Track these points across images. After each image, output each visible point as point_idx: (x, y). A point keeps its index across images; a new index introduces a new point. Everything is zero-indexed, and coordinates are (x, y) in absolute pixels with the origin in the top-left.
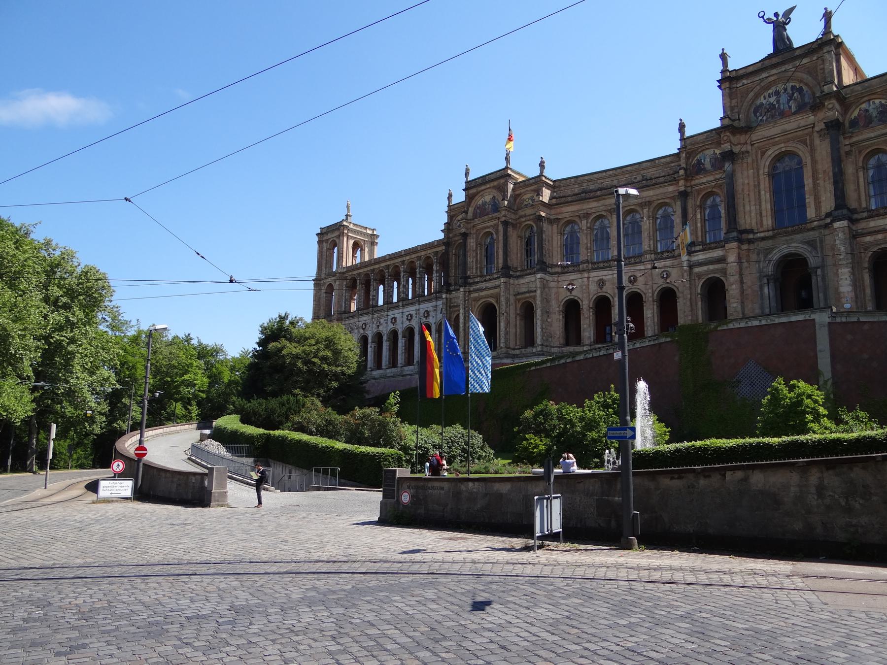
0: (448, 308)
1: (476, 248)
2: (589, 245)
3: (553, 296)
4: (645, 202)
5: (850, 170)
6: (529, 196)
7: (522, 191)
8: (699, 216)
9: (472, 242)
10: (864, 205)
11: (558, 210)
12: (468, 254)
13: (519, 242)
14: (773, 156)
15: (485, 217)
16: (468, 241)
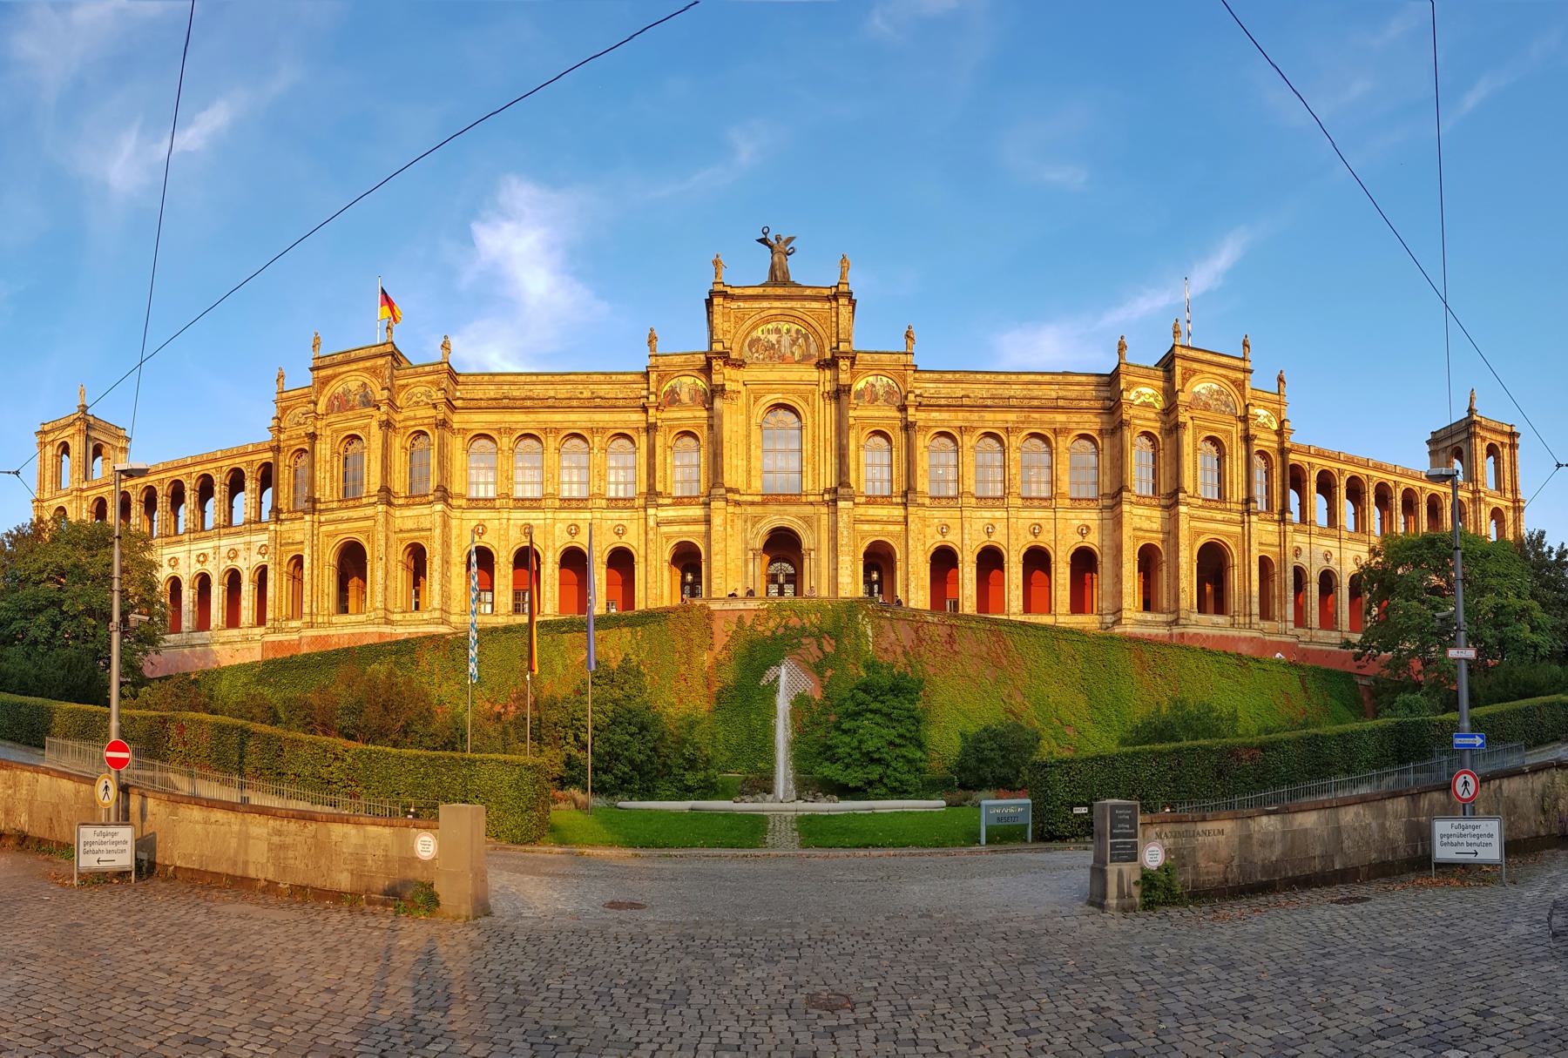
0: (278, 546)
1: (332, 458)
2: (510, 473)
3: (453, 541)
4: (597, 429)
5: (852, 446)
6: (422, 389)
7: (410, 381)
8: (669, 461)
9: (323, 449)
10: (862, 489)
11: (466, 417)
12: (317, 467)
13: (403, 454)
14: (768, 405)
15: (350, 413)
16: (318, 447)
